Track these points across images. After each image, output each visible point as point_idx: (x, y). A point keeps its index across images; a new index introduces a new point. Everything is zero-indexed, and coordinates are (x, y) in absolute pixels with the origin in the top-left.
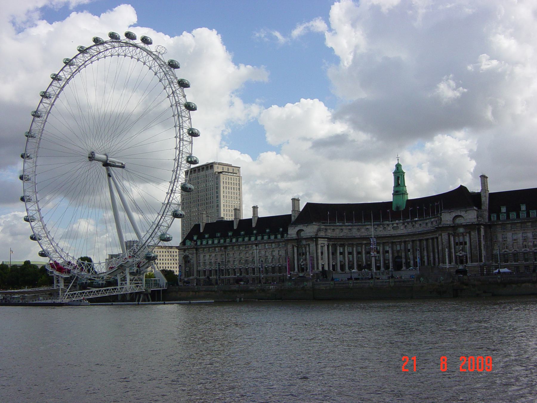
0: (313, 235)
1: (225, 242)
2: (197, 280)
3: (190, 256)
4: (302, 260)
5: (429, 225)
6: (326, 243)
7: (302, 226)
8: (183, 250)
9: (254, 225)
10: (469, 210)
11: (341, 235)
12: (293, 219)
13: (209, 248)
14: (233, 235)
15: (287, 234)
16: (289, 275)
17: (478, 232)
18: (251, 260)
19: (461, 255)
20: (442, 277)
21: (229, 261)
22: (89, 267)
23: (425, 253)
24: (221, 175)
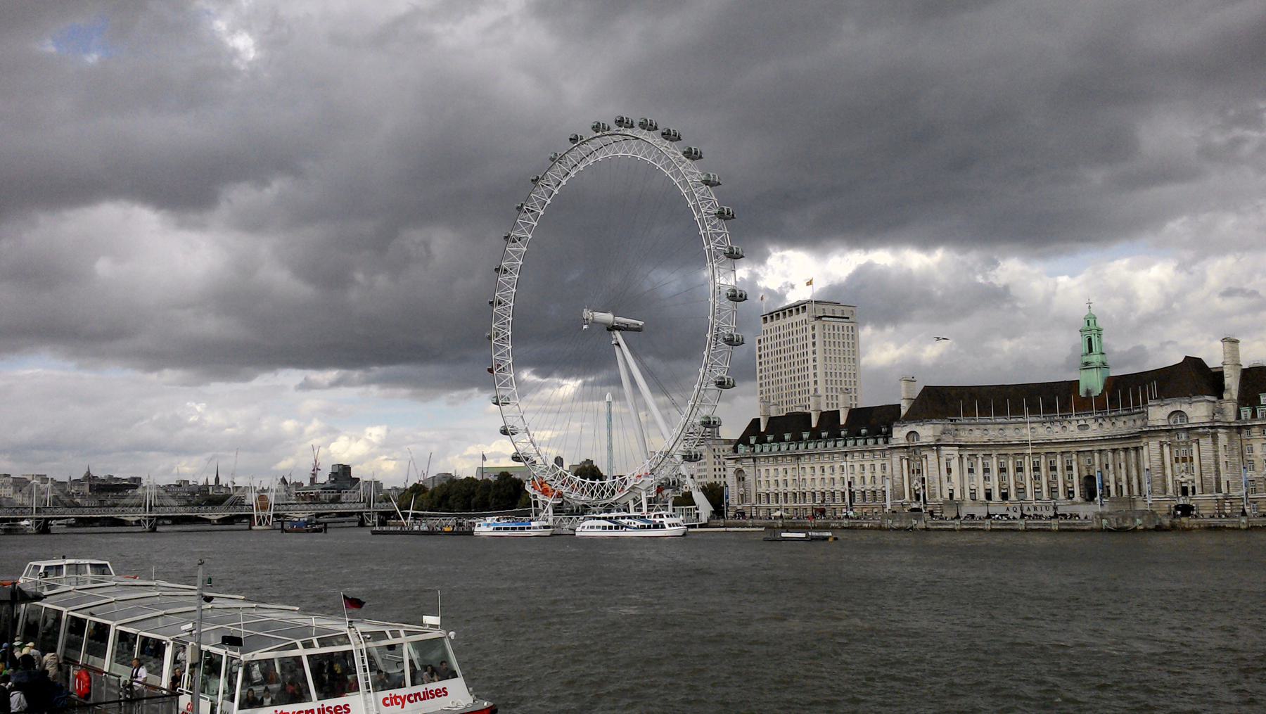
0: (931, 440)
1: (798, 448)
2: (756, 508)
3: (744, 469)
6: (956, 454)
7: (914, 425)
8: (733, 461)
9: (843, 421)
10: (1195, 402)
12: (903, 412)
14: (811, 438)
17: (1213, 441)
18: (839, 478)
19: (1183, 480)
20: (1138, 520)
21: (805, 479)
23: (1134, 473)
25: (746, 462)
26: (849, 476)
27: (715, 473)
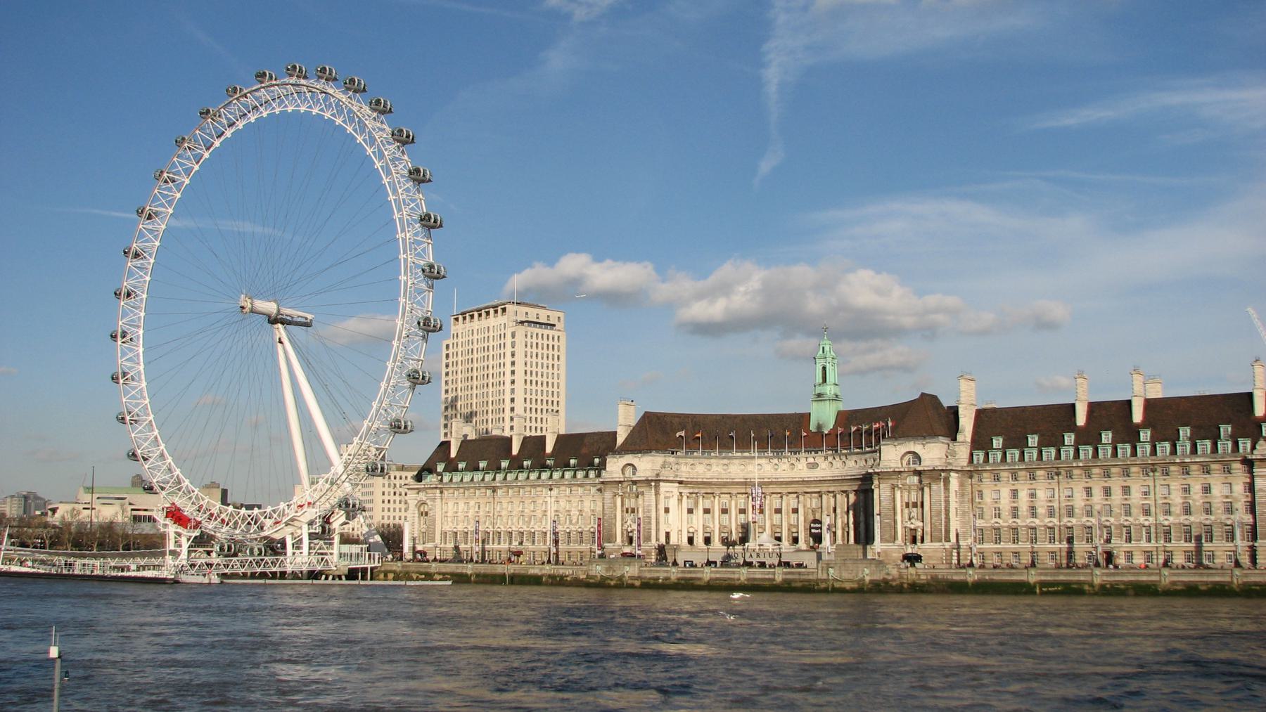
0: (650, 475)
1: (494, 479)
3: (428, 502)
4: (628, 523)
5: (862, 463)
8: (417, 491)
9: (549, 449)
11: (709, 475)
12: (620, 440)
13: (465, 488)
15: (605, 469)
16: (600, 552)
17: (944, 485)
19: (912, 527)
22: (237, 518)
24: (520, 327)
25: (430, 494)
26: (553, 514)
27: (383, 505)
